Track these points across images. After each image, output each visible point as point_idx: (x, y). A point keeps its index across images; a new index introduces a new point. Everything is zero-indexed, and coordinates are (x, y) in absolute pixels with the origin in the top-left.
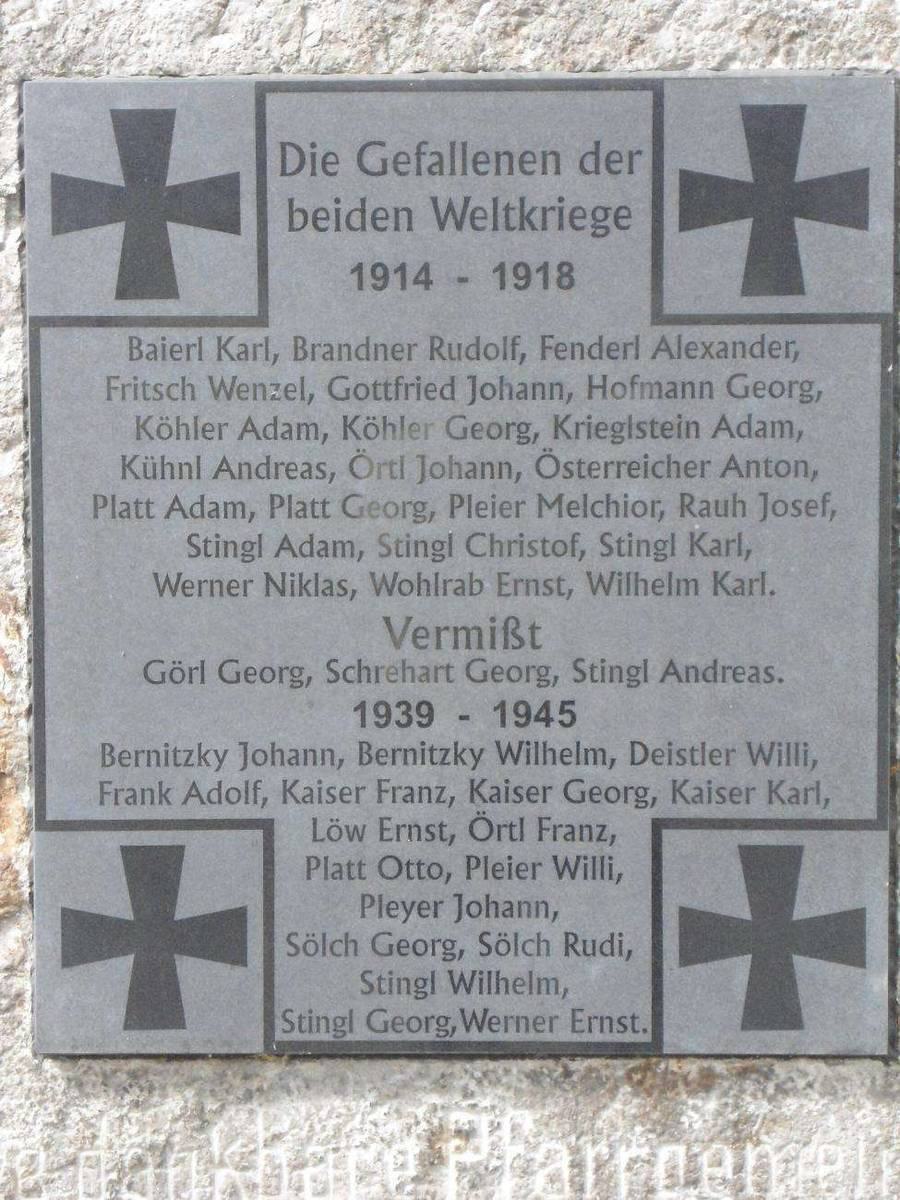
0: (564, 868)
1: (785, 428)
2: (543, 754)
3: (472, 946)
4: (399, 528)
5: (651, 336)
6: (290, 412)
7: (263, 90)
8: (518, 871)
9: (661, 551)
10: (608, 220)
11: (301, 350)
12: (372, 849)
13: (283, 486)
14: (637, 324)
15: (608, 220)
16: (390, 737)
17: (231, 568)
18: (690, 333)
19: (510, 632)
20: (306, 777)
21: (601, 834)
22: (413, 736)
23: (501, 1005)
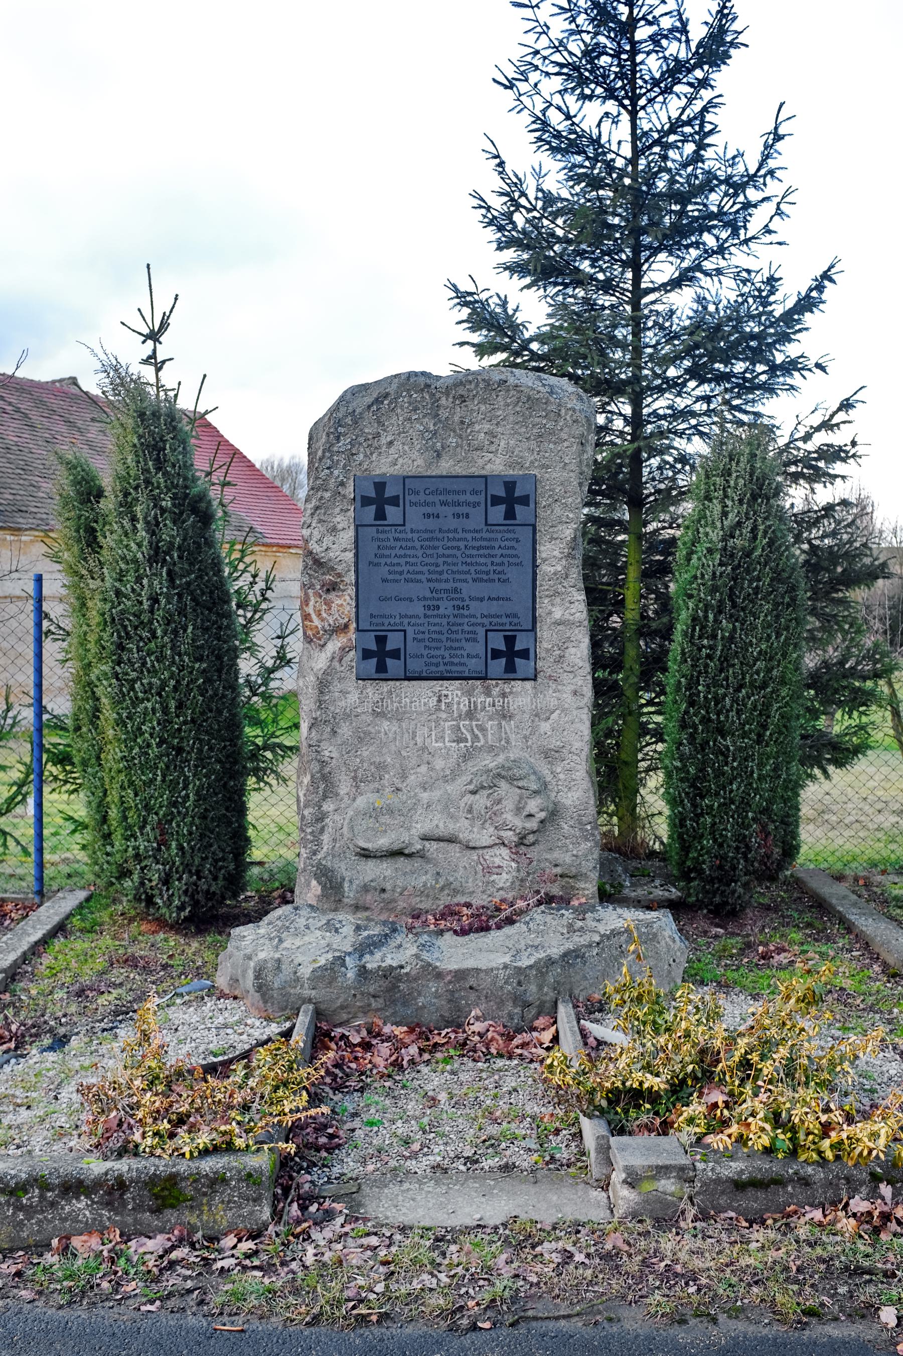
0: (467, 640)
1: (513, 548)
2: (463, 616)
3: (447, 656)
4: (432, 568)
5: (485, 528)
6: (409, 544)
7: (405, 478)
8: (457, 640)
9: (488, 573)
10: (476, 505)
11: (412, 531)
12: (427, 636)
13: (408, 560)
14: (483, 526)
15: (476, 505)
16: (430, 613)
17: (398, 577)
18: (493, 528)
19: (456, 590)
20: (413, 621)
21: (475, 633)
22: (436, 612)
23: (454, 668)
